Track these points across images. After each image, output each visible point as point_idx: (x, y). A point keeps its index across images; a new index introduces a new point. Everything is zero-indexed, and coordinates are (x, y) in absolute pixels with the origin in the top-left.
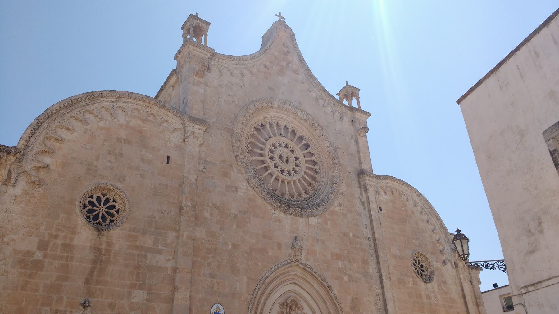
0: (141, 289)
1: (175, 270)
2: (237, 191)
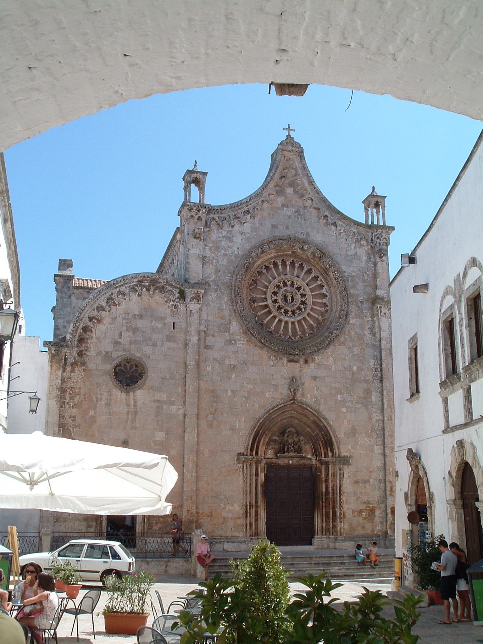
0: (161, 431)
1: (185, 415)
2: (235, 342)
